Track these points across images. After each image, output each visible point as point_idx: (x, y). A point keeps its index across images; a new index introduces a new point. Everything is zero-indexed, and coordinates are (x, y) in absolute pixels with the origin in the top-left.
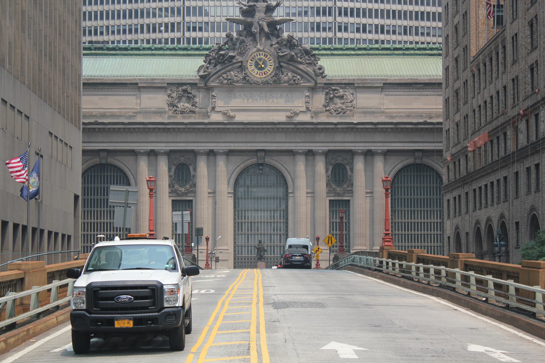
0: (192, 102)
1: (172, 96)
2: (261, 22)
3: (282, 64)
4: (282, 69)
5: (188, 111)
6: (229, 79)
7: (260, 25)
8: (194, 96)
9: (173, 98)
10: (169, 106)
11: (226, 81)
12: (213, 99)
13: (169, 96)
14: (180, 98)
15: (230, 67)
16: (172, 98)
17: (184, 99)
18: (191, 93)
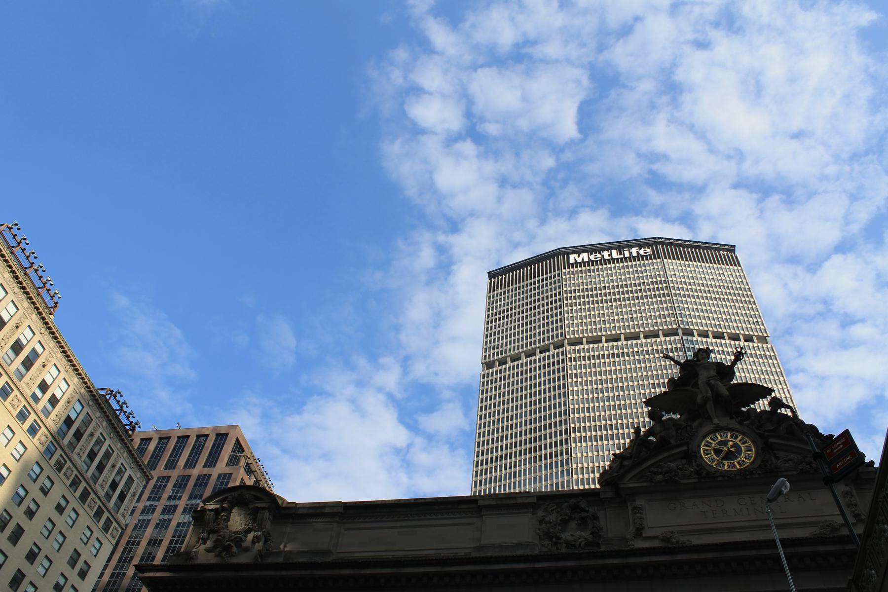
0: (590, 526)
1: (547, 519)
2: (712, 382)
3: (771, 440)
4: (776, 452)
5: (583, 544)
6: (667, 472)
7: (712, 387)
8: (595, 518)
9: (551, 523)
10: (540, 539)
11: (661, 476)
12: (635, 513)
13: (541, 522)
14: (564, 523)
15: (666, 455)
16: (546, 523)
17: (572, 525)
18: (588, 512)
